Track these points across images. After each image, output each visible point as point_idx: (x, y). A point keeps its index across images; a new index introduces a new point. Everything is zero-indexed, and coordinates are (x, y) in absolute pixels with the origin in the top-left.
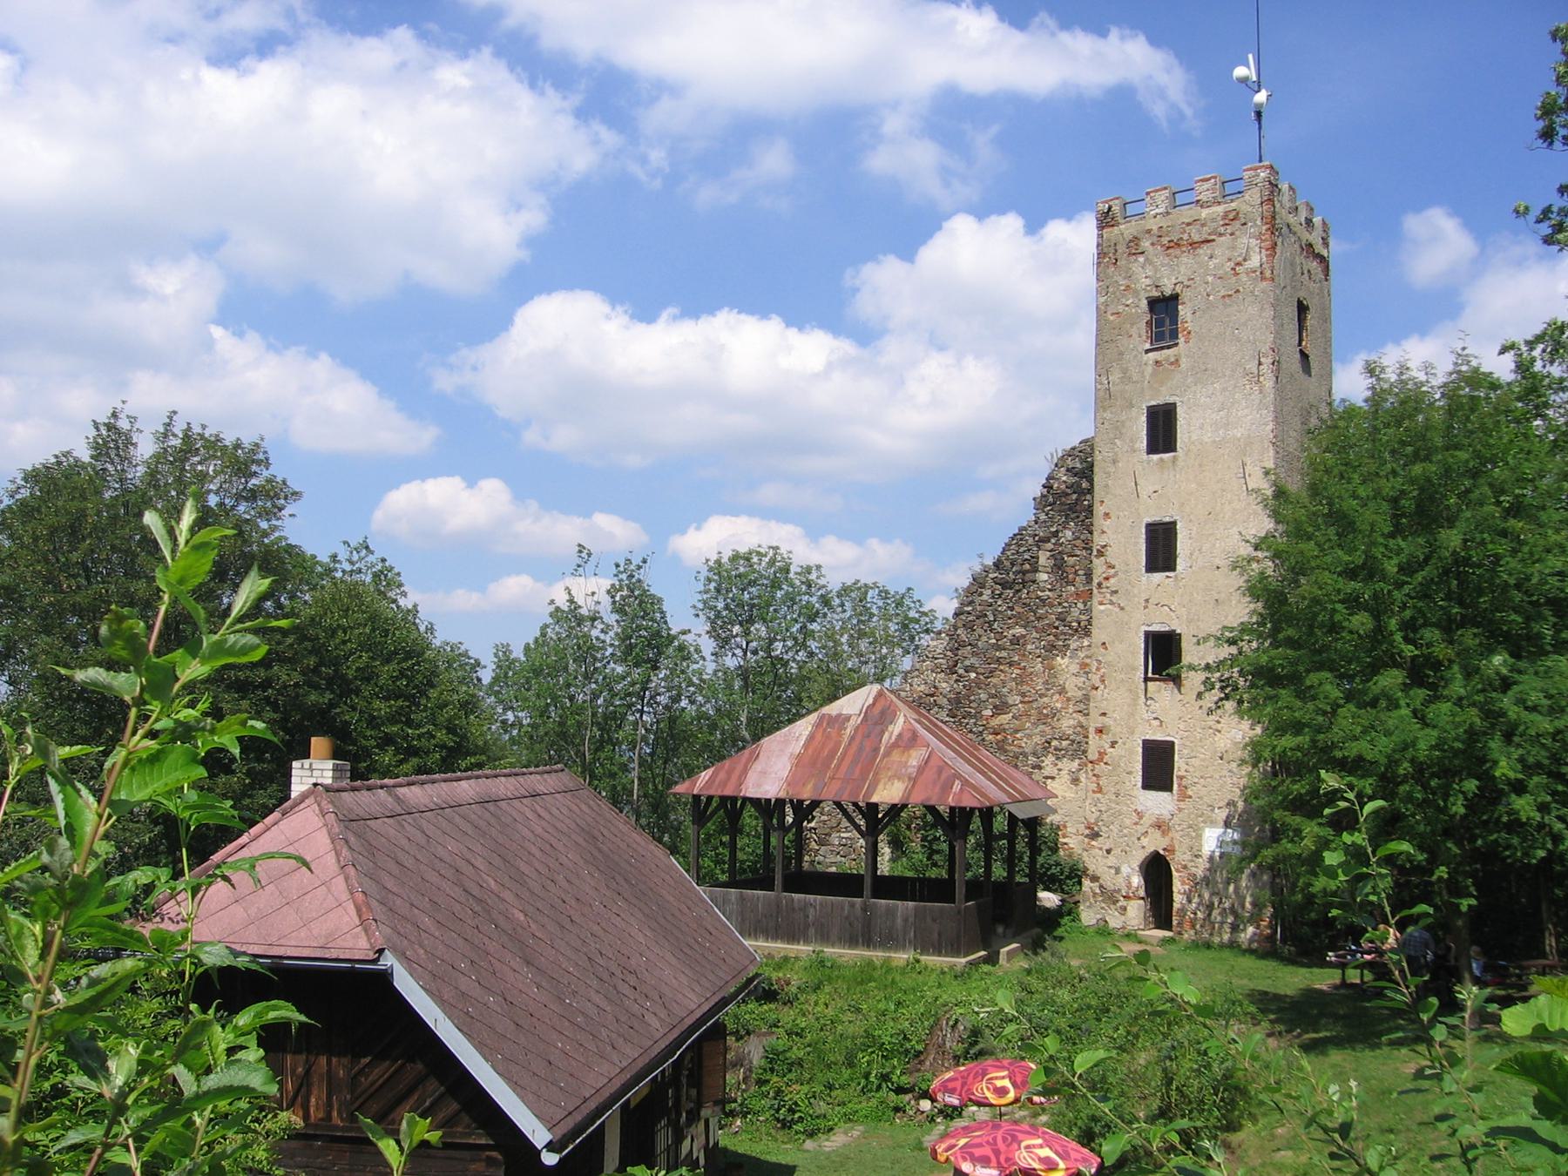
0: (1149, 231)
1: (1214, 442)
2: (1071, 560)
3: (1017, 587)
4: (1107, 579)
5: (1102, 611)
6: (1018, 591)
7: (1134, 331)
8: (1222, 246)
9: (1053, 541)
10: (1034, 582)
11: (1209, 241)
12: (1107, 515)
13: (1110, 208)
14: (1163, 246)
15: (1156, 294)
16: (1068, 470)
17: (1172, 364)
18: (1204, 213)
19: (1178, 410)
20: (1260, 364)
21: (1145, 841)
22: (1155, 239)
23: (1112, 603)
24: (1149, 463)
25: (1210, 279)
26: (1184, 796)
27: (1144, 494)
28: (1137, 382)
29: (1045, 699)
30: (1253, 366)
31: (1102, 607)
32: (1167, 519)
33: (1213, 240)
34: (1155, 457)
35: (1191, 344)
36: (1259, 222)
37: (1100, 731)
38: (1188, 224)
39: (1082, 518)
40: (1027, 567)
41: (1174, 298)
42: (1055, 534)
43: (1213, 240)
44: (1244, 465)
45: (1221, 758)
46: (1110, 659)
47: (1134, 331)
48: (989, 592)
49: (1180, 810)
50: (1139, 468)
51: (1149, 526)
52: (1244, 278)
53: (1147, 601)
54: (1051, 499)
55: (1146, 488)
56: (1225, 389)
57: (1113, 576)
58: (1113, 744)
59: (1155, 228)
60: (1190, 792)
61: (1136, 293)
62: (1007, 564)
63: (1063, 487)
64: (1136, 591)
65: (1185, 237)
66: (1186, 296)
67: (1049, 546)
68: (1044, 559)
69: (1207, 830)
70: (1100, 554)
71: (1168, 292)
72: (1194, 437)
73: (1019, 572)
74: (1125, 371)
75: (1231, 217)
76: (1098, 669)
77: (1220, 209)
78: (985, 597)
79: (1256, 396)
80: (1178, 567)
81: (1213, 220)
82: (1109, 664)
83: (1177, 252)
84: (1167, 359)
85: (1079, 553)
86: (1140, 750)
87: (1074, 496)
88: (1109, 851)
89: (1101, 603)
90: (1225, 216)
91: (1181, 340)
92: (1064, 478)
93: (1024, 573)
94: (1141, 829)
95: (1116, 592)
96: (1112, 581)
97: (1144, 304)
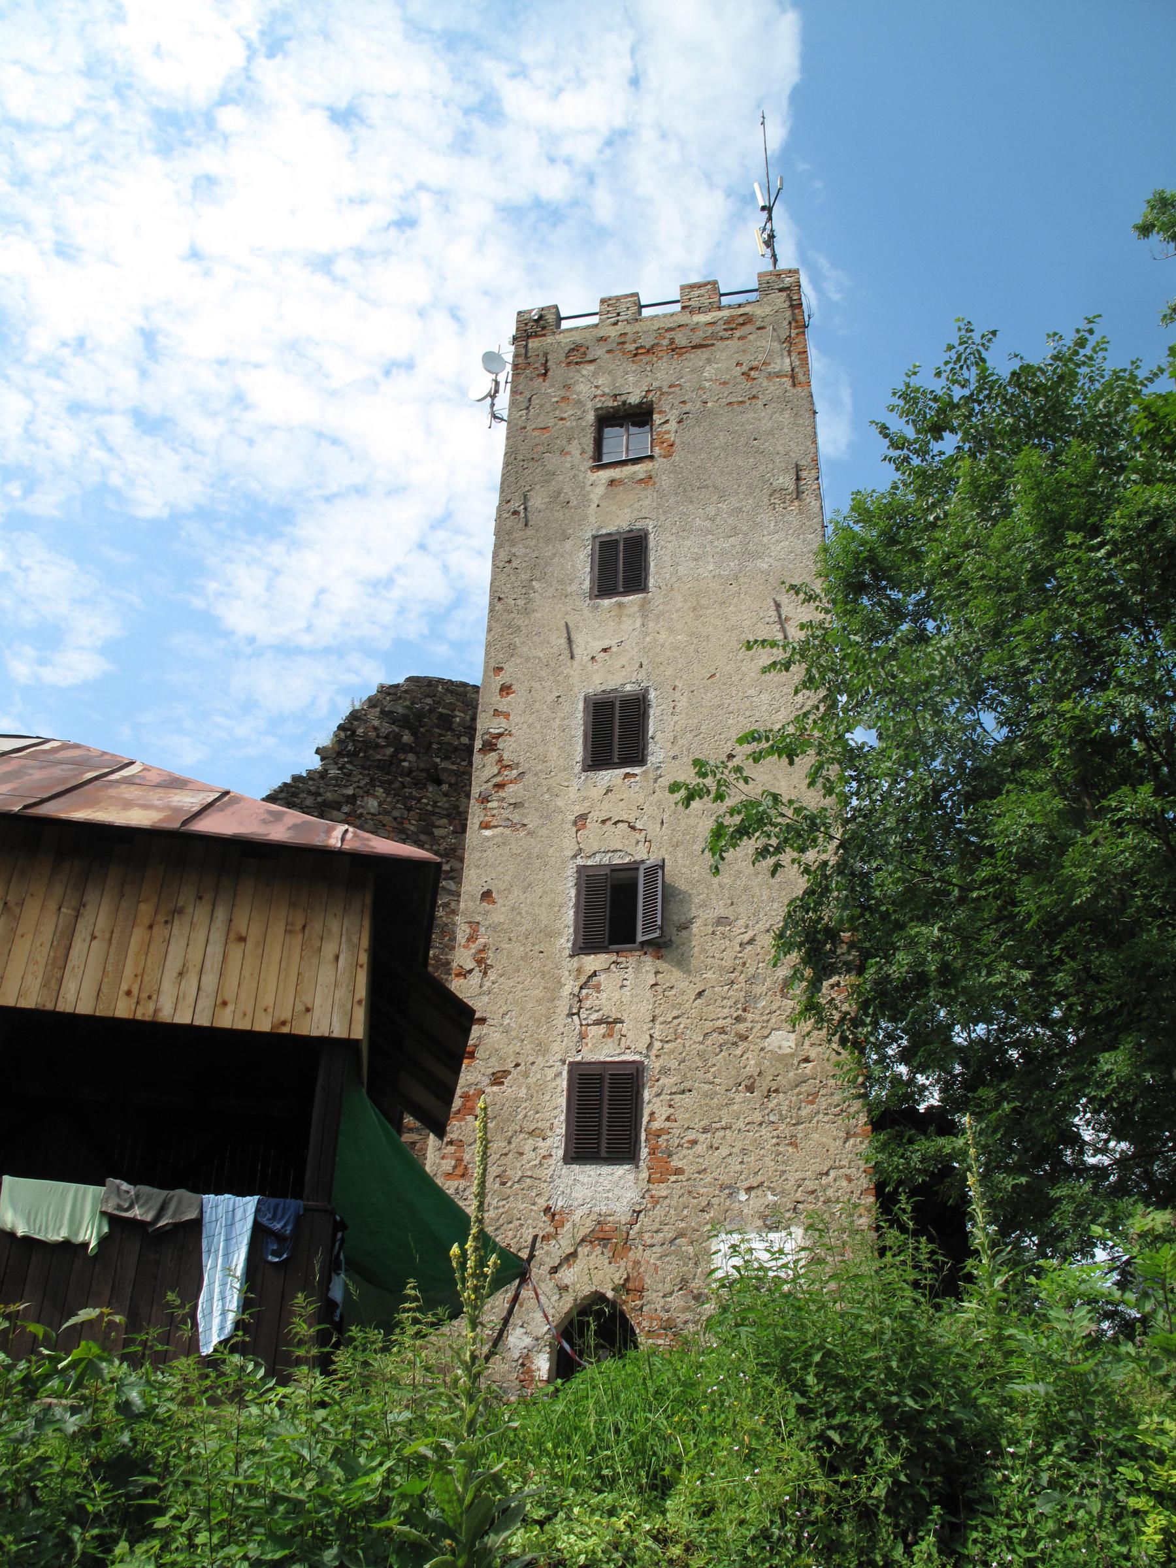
4: (500, 786)
5: (488, 839)
9: (346, 809)
14: (624, 353)
16: (382, 712)
20: (798, 479)
21: (568, 1275)
26: (662, 1171)
31: (487, 833)
33: (713, 345)
34: (606, 602)
35: (676, 458)
39: (396, 785)
42: (351, 800)
43: (713, 345)
44: (778, 606)
45: (750, 1089)
49: (656, 1201)
51: (586, 699)
53: (583, 817)
54: (350, 747)
55: (587, 644)
60: (675, 1163)
64: (560, 803)
70: (489, 747)
71: (634, 399)
72: (682, 570)
75: (741, 320)
76: (472, 938)
80: (651, 759)
82: (494, 928)
84: (631, 477)
86: (564, 1084)
89: (486, 826)
92: (376, 723)
96: (511, 788)
97: (591, 417)
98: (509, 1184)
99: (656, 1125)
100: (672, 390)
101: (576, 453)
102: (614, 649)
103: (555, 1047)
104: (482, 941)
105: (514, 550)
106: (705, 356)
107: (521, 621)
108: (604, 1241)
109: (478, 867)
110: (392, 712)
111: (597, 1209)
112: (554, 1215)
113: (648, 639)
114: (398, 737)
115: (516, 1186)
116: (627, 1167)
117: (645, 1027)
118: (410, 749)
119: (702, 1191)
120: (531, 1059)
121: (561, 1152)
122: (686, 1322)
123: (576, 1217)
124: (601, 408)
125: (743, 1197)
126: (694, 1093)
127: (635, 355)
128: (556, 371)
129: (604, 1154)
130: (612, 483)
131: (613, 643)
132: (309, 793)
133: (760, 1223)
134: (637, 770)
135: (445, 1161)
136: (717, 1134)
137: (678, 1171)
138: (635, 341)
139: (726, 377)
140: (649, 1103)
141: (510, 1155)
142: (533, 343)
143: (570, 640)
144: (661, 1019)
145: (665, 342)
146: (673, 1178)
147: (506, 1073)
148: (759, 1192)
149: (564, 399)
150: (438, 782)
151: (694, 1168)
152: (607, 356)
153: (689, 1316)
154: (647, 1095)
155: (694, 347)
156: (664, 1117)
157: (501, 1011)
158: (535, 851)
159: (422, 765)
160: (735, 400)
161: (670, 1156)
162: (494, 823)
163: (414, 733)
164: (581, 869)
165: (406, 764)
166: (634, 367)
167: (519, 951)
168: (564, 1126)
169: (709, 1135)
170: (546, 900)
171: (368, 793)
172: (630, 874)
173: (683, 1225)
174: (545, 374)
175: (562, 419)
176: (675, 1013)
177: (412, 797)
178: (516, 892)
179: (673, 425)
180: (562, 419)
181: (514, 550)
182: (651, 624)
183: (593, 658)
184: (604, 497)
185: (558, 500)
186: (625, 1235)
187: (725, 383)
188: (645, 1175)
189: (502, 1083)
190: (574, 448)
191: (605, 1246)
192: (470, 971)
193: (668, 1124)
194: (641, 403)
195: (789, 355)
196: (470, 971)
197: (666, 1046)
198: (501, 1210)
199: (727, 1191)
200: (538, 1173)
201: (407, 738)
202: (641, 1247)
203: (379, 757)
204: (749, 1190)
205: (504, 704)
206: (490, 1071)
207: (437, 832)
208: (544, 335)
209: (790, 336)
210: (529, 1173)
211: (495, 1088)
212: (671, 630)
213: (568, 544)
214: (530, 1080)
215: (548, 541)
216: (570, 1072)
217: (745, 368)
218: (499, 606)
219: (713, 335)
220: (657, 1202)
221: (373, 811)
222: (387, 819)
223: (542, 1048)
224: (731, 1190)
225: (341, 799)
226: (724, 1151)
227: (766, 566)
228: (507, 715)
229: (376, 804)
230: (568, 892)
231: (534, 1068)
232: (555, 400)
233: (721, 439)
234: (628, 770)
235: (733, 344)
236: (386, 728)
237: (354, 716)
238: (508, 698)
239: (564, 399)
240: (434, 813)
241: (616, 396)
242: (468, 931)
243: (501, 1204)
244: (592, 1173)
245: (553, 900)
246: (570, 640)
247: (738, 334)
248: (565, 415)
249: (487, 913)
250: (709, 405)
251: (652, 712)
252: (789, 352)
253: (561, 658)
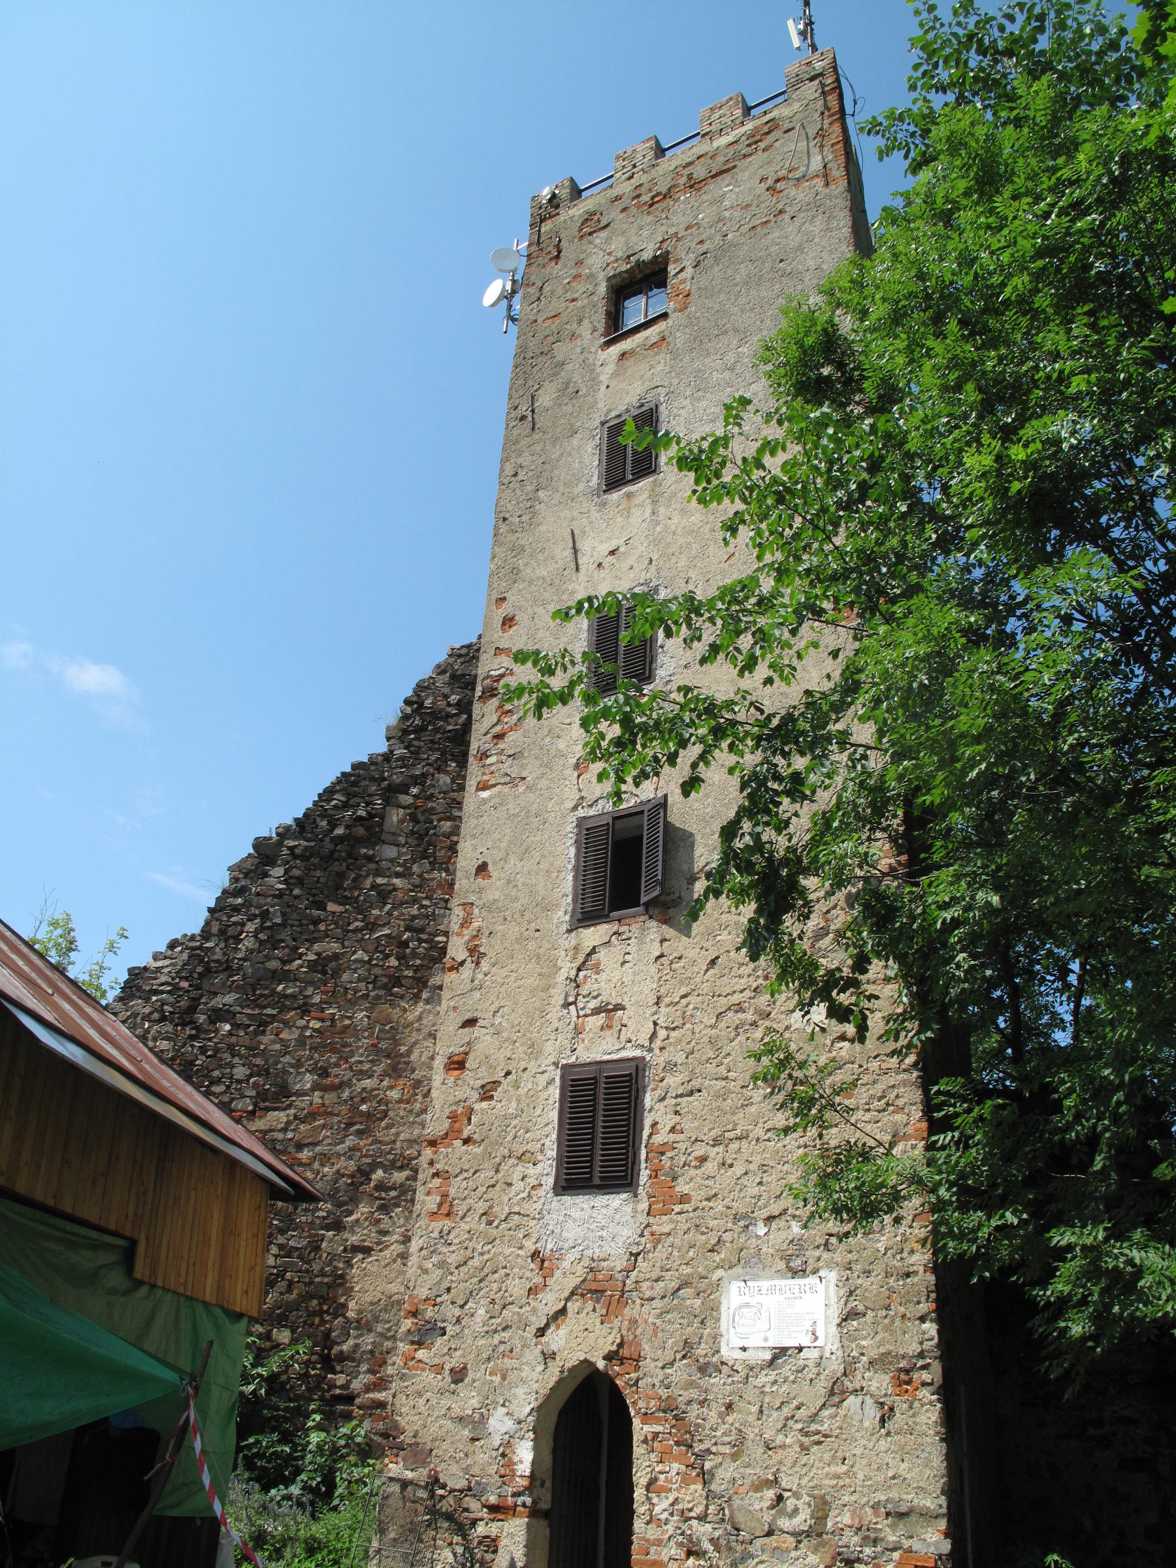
4: (500, 737)
21: (557, 1339)
29: (368, 1083)
31: (485, 794)
33: (735, 167)
34: (615, 496)
37: (457, 1064)
43: (735, 167)
49: (657, 1239)
55: (593, 548)
58: (487, 1093)
60: (682, 1187)
67: (406, 799)
69: (735, 1286)
75: (766, 129)
76: (465, 924)
82: (488, 907)
86: (555, 1092)
88: (459, 1375)
94: (550, 1301)
96: (511, 737)
98: (495, 1224)
99: (658, 1139)
102: (622, 549)
103: (549, 1047)
104: (476, 925)
105: (520, 460)
108: (598, 1293)
109: (473, 836)
110: (464, 675)
111: (589, 1253)
112: (543, 1261)
113: (659, 529)
115: (504, 1225)
116: (624, 1196)
117: (648, 1012)
119: (712, 1223)
120: (523, 1064)
121: (551, 1181)
122: (689, 1402)
123: (566, 1264)
124: (614, 276)
125: (761, 1230)
126: (704, 1093)
127: (651, 205)
129: (597, 1181)
130: (623, 355)
132: (373, 779)
133: (782, 1265)
135: (430, 1198)
136: (731, 1146)
137: (684, 1199)
140: (650, 1111)
141: (497, 1188)
142: (546, 227)
143: (575, 551)
144: (667, 1000)
146: (677, 1208)
147: (496, 1083)
148: (781, 1223)
151: (703, 1193)
153: (694, 1394)
154: (648, 1100)
155: (713, 177)
156: (668, 1128)
157: (493, 1008)
161: (674, 1179)
162: (492, 782)
164: (581, 821)
166: (650, 219)
167: (514, 931)
168: (555, 1147)
169: (720, 1149)
170: (545, 865)
171: (439, 770)
172: (634, 821)
173: (688, 1270)
174: (558, 257)
175: (573, 300)
176: (683, 991)
178: (513, 860)
179: (689, 271)
182: (662, 510)
183: (600, 565)
184: (614, 375)
185: (570, 393)
186: (620, 1285)
187: (747, 206)
188: (644, 1206)
189: (491, 1098)
190: (585, 330)
191: (598, 1301)
192: (462, 963)
193: (672, 1137)
194: (655, 257)
195: (821, 151)
196: (462, 963)
197: (673, 1034)
198: (486, 1257)
199: (742, 1223)
200: (528, 1208)
202: (638, 1301)
203: (450, 728)
204: (770, 1219)
206: (479, 1083)
209: (821, 129)
210: (516, 1209)
211: (485, 1104)
214: (522, 1091)
215: (555, 441)
216: (562, 1077)
217: (770, 182)
218: (503, 528)
220: (659, 1241)
221: (444, 788)
223: (534, 1050)
224: (745, 1220)
225: (409, 781)
226: (738, 1170)
229: (448, 780)
230: (567, 852)
231: (525, 1075)
232: (566, 281)
233: (743, 271)
235: (760, 157)
237: (420, 688)
238: (511, 632)
241: (629, 257)
242: (461, 914)
243: (486, 1248)
244: (585, 1206)
245: (552, 864)
246: (575, 551)
247: (762, 145)
248: (576, 295)
249: (481, 890)
252: (822, 146)
253: (566, 573)
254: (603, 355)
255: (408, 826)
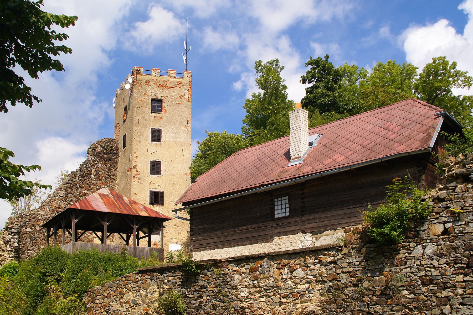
0: (153, 80)
1: (173, 141)
2: (101, 173)
3: (86, 178)
5: (135, 184)
6: (86, 179)
7: (147, 107)
8: (177, 90)
9: (96, 166)
10: (90, 177)
11: (172, 87)
12: (137, 157)
13: (140, 70)
14: (157, 85)
15: (154, 97)
17: (160, 118)
18: (171, 80)
19: (162, 131)
22: (155, 82)
23: (138, 182)
24: (152, 144)
25: (173, 98)
27: (150, 153)
28: (148, 121)
30: (186, 123)
31: (135, 183)
32: (158, 160)
33: (174, 88)
34: (154, 143)
36: (188, 86)
38: (166, 81)
40: (89, 172)
41: (161, 101)
42: (96, 164)
43: (174, 88)
44: (183, 149)
46: (138, 198)
47: (147, 107)
48: (78, 178)
50: (148, 145)
51: (151, 161)
52: (183, 99)
55: (151, 151)
56: (177, 128)
57: (139, 174)
59: (155, 79)
61: (148, 96)
62: (83, 170)
63: (99, 151)
64: (147, 179)
65: (165, 84)
66: (165, 100)
68: (93, 171)
70: (134, 168)
71: (159, 98)
72: (167, 139)
73: (86, 174)
74: (144, 117)
77: (177, 80)
78: (76, 179)
79: (186, 131)
81: (174, 82)
83: (162, 88)
84: (159, 116)
85: (103, 171)
87: (102, 154)
89: (134, 182)
90: (178, 82)
91: (163, 112)
92: (99, 148)
93: (88, 174)
95: (140, 179)
96: (138, 176)
100: (166, 97)
101: (148, 108)
102: (155, 153)
106: (173, 90)
107: (139, 144)
114: (104, 151)
118: (106, 154)
127: (159, 86)
128: (143, 86)
131: (155, 151)
134: (159, 175)
138: (159, 82)
139: (176, 97)
145: (165, 84)
149: (145, 94)
150: (111, 160)
152: (154, 85)
158: (143, 187)
159: (108, 157)
160: (177, 103)
163: (106, 150)
165: (105, 157)
170: (145, 195)
177: (107, 164)
180: (145, 99)
181: (137, 128)
182: (162, 149)
184: (153, 120)
201: (105, 151)
205: (136, 160)
207: (111, 171)
208: (140, 75)
212: (165, 150)
213: (147, 129)
217: (180, 96)
219: (174, 85)
222: (103, 168)
227: (181, 141)
228: (137, 162)
234: (158, 175)
236: (102, 149)
239: (145, 94)
240: (110, 167)
247: (179, 86)
249: (135, 197)
250: (173, 103)
251: (162, 165)
254: (151, 115)
255: (95, 173)
